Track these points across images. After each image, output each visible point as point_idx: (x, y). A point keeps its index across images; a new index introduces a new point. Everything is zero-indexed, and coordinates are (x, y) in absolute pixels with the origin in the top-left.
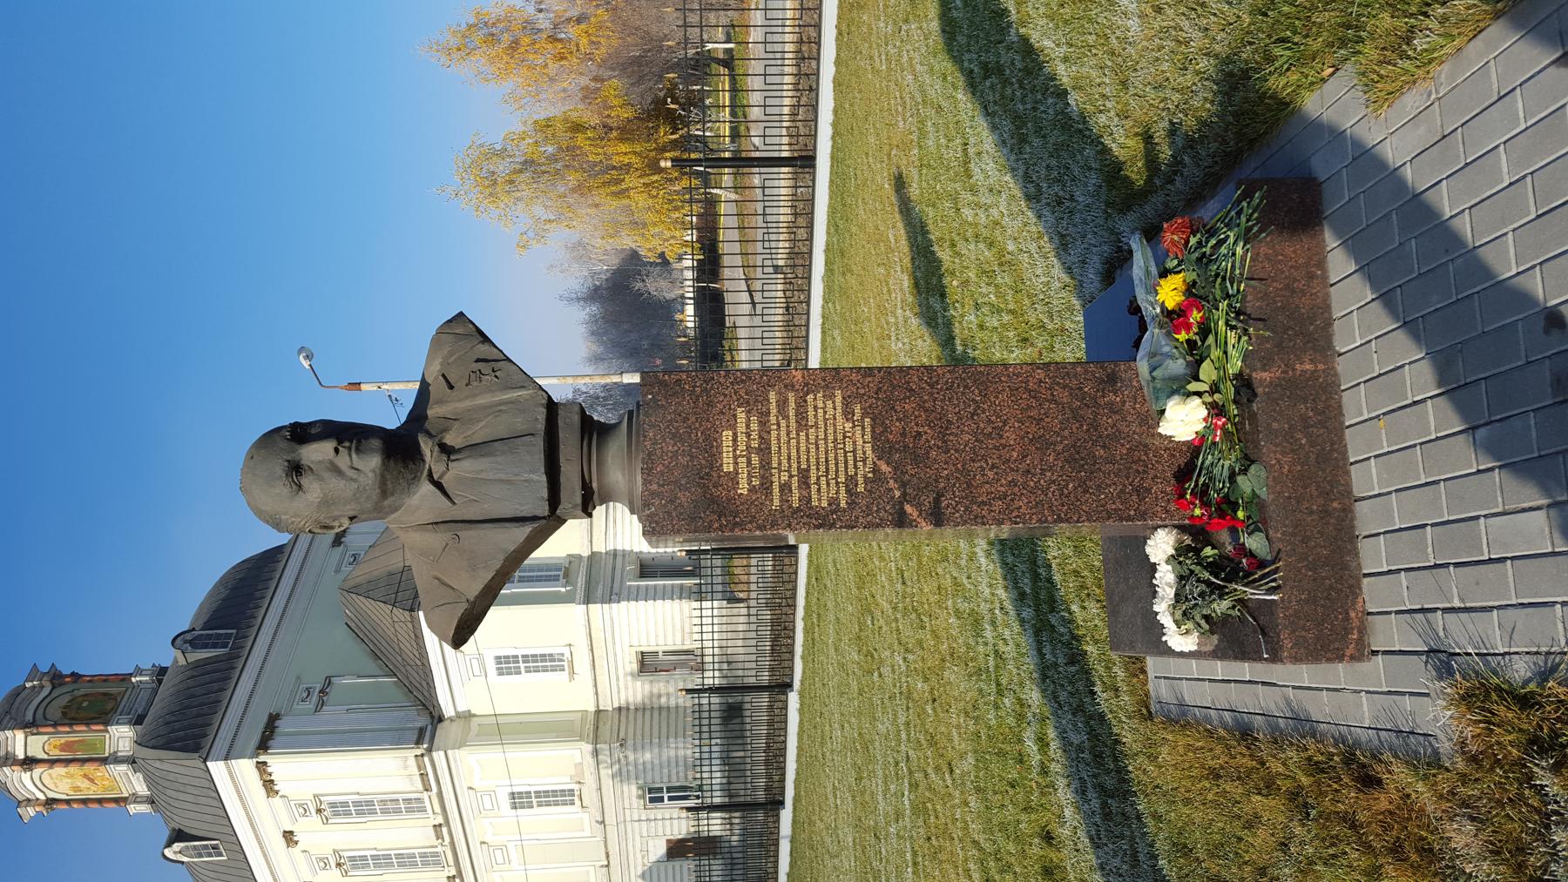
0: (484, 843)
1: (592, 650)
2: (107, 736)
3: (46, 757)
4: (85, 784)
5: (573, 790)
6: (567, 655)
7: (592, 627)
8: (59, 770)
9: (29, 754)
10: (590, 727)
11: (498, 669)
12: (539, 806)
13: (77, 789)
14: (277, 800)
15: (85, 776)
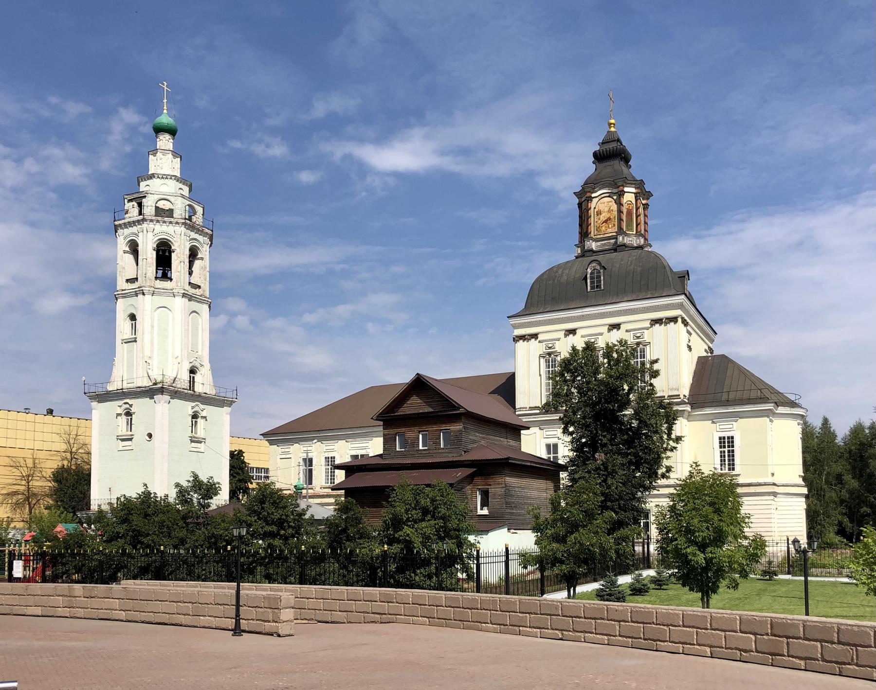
3: (625, 202)
4: (603, 217)
11: (724, 438)
13: (599, 213)
14: (647, 324)
15: (609, 219)
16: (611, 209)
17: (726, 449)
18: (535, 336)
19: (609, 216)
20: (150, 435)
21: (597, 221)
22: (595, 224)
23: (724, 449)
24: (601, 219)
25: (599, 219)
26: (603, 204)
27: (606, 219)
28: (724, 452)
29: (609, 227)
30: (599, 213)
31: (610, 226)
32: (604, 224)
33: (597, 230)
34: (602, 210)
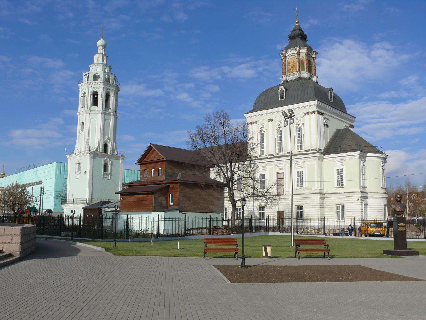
0: (285, 164)
1: (345, 193)
2: (305, 71)
3: (300, 57)
4: (291, 65)
5: (303, 187)
6: (343, 187)
7: (353, 193)
8: (296, 60)
9: (301, 54)
10: (322, 191)
12: (298, 178)
13: (289, 63)
15: (294, 66)
16: (295, 61)
17: (340, 175)
18: (256, 122)
19: (293, 64)
20: (85, 172)
21: (288, 67)
22: (288, 68)
23: (339, 175)
24: (290, 66)
25: (290, 66)
26: (291, 59)
27: (292, 65)
28: (339, 176)
29: (294, 69)
30: (289, 63)
31: (294, 69)
32: (292, 68)
33: (289, 71)
34: (290, 62)
